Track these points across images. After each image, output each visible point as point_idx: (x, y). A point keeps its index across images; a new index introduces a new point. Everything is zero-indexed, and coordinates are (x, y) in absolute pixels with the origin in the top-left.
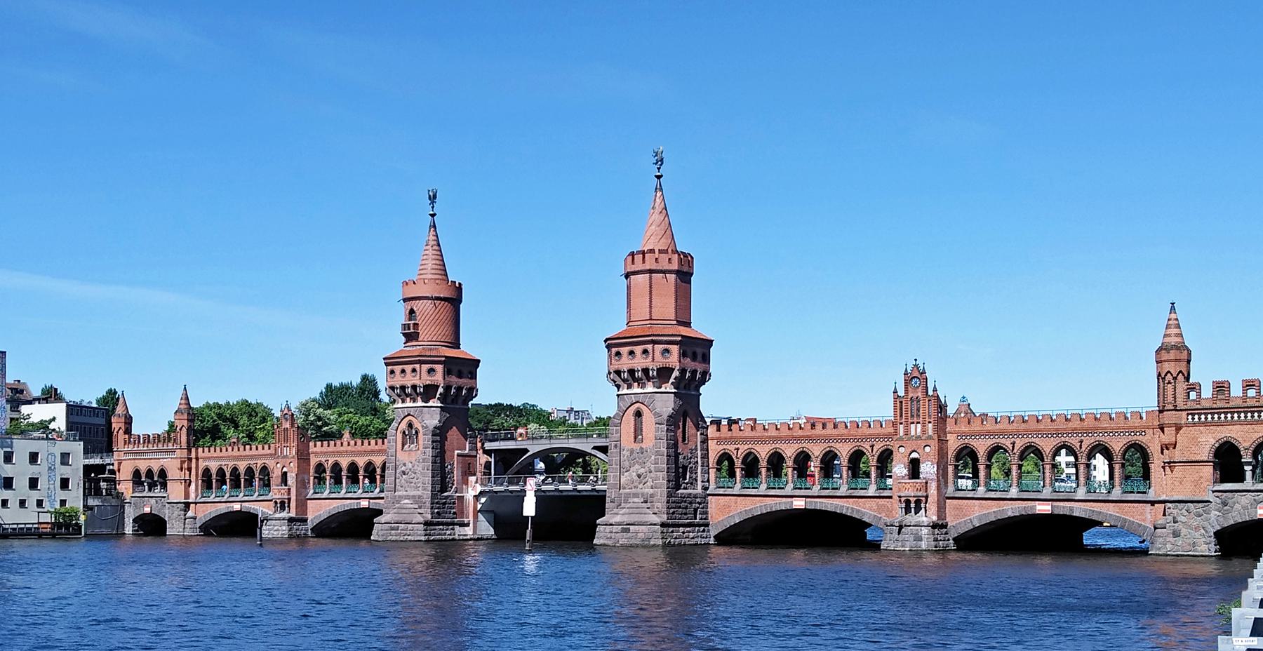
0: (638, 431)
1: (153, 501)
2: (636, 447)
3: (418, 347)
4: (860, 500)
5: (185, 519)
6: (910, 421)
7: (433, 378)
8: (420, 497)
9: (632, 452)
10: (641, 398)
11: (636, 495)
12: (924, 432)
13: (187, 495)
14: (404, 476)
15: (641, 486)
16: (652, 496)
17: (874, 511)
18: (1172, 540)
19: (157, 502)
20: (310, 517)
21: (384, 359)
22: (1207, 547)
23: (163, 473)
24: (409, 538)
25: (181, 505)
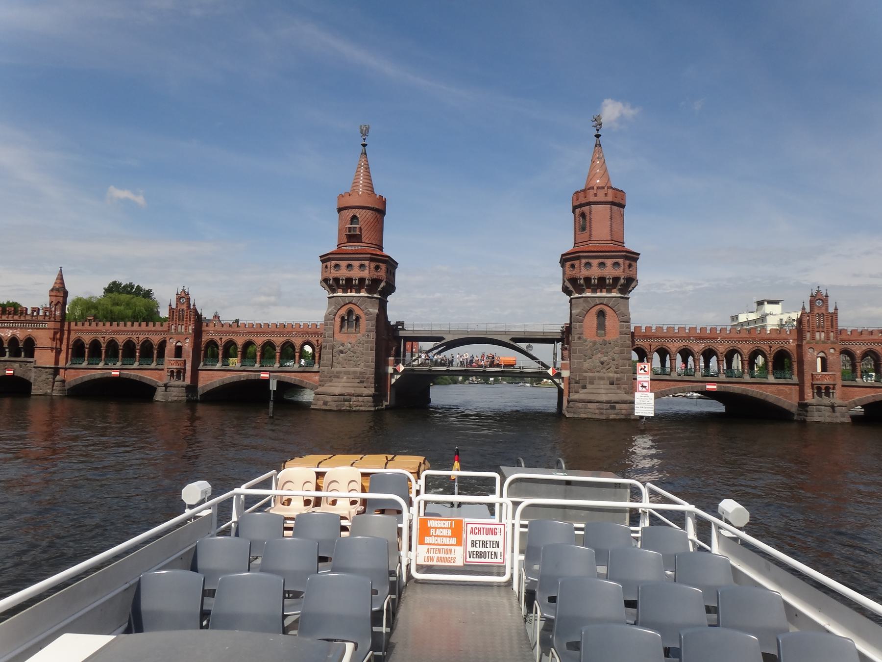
0: (601, 326)
1: (16, 365)
2: (599, 340)
3: (360, 247)
4: (763, 386)
7: (378, 274)
8: (361, 373)
9: (595, 343)
11: (601, 378)
16: (618, 379)
19: (21, 366)
20: (200, 385)
21: (321, 257)
24: (361, 408)
25: (50, 370)
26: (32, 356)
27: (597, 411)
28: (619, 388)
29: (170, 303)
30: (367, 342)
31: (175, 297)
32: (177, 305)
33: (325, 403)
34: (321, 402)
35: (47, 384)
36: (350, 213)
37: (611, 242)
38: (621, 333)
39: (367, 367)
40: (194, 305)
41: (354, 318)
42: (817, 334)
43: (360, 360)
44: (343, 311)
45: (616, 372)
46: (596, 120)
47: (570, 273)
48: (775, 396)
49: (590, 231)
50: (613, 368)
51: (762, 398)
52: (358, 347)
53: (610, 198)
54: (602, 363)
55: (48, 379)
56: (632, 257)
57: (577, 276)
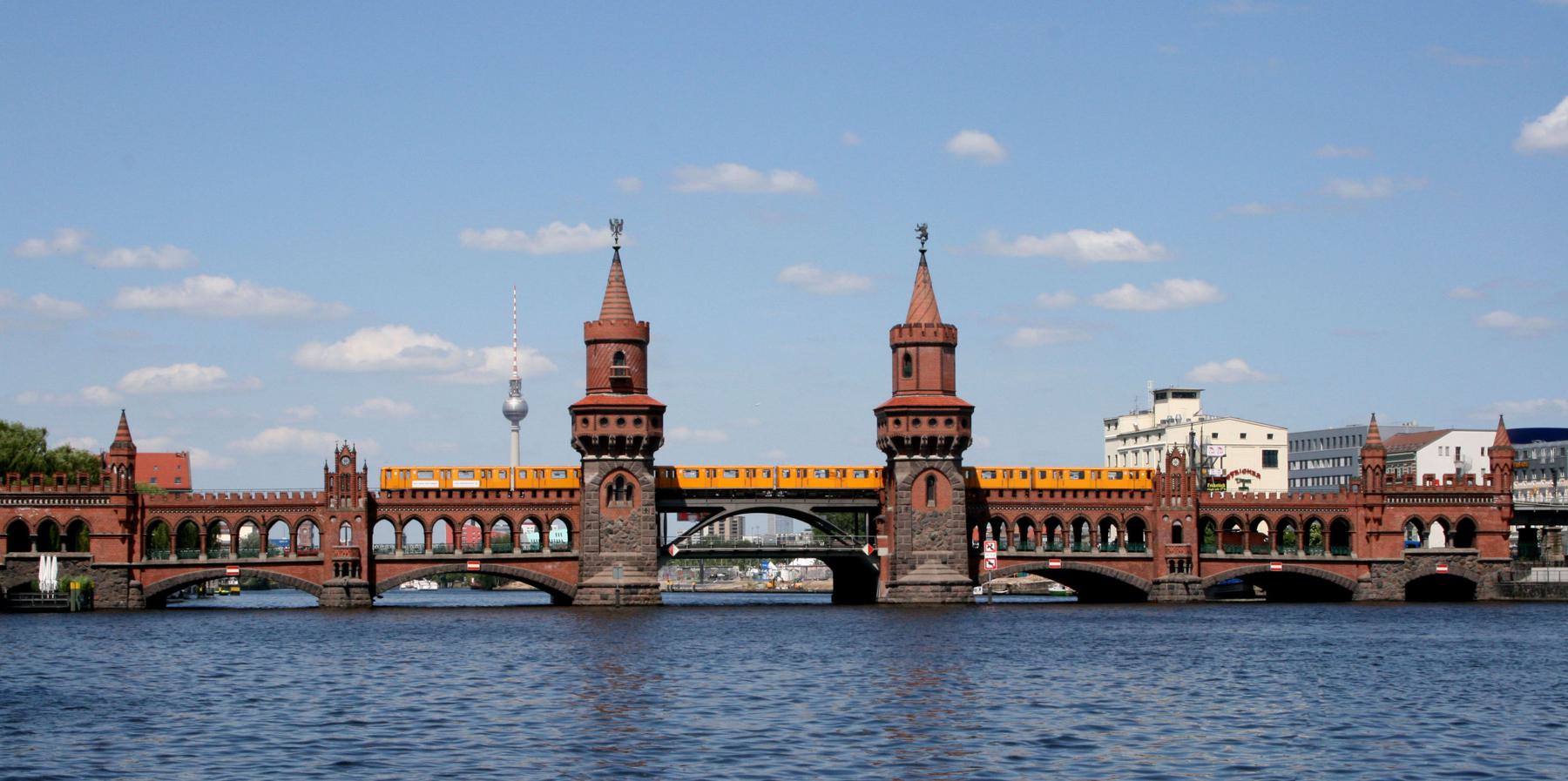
0: (930, 494)
5: (129, 587)
6: (1172, 493)
8: (639, 559)
9: (924, 516)
10: (936, 465)
11: (931, 557)
12: (1184, 503)
13: (130, 560)
14: (611, 536)
15: (935, 547)
16: (951, 558)
17: (1126, 570)
18: (1377, 590)
22: (1400, 595)
23: (77, 526)
26: (88, 550)
27: (931, 594)
28: (953, 568)
29: (326, 466)
30: (645, 519)
31: (333, 456)
32: (337, 468)
33: (604, 598)
34: (598, 596)
35: (117, 591)
36: (613, 348)
37: (940, 393)
38: (954, 503)
39: (649, 550)
40: (365, 469)
41: (625, 487)
42: (1173, 499)
43: (635, 542)
44: (610, 479)
45: (949, 549)
46: (920, 230)
47: (893, 429)
48: (1126, 573)
49: (918, 379)
50: (945, 545)
51: (1113, 575)
52: (633, 524)
53: (940, 339)
54: (933, 539)
55: (119, 583)
56: (965, 413)
57: (905, 434)
